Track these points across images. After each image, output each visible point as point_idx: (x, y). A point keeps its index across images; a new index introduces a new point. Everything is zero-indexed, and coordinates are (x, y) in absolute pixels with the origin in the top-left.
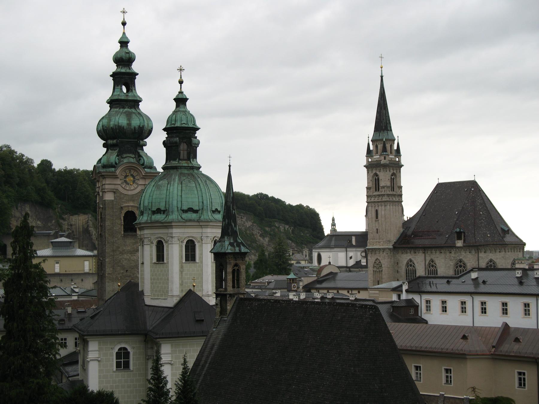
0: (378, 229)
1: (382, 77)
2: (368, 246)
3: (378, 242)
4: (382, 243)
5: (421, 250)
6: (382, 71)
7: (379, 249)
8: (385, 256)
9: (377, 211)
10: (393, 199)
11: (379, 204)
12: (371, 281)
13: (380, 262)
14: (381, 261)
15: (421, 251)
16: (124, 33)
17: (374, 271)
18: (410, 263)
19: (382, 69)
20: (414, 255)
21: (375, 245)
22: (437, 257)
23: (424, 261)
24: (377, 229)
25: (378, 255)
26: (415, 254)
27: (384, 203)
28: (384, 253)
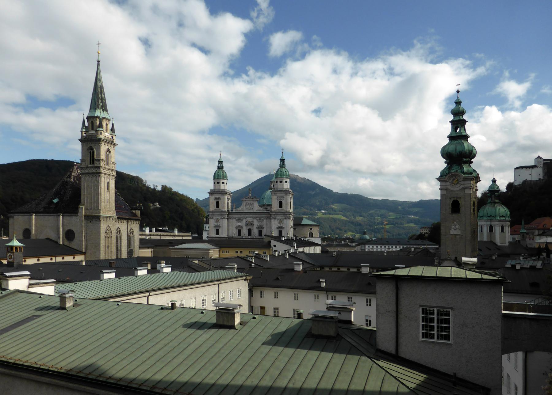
2: (101, 213)
3: (109, 211)
4: (112, 212)
5: (125, 220)
7: (110, 217)
8: (114, 224)
10: (85, 171)
13: (110, 229)
15: (125, 222)
16: (458, 97)
18: (119, 231)
20: (121, 224)
22: (134, 227)
25: (109, 222)
26: (121, 223)
28: (114, 222)
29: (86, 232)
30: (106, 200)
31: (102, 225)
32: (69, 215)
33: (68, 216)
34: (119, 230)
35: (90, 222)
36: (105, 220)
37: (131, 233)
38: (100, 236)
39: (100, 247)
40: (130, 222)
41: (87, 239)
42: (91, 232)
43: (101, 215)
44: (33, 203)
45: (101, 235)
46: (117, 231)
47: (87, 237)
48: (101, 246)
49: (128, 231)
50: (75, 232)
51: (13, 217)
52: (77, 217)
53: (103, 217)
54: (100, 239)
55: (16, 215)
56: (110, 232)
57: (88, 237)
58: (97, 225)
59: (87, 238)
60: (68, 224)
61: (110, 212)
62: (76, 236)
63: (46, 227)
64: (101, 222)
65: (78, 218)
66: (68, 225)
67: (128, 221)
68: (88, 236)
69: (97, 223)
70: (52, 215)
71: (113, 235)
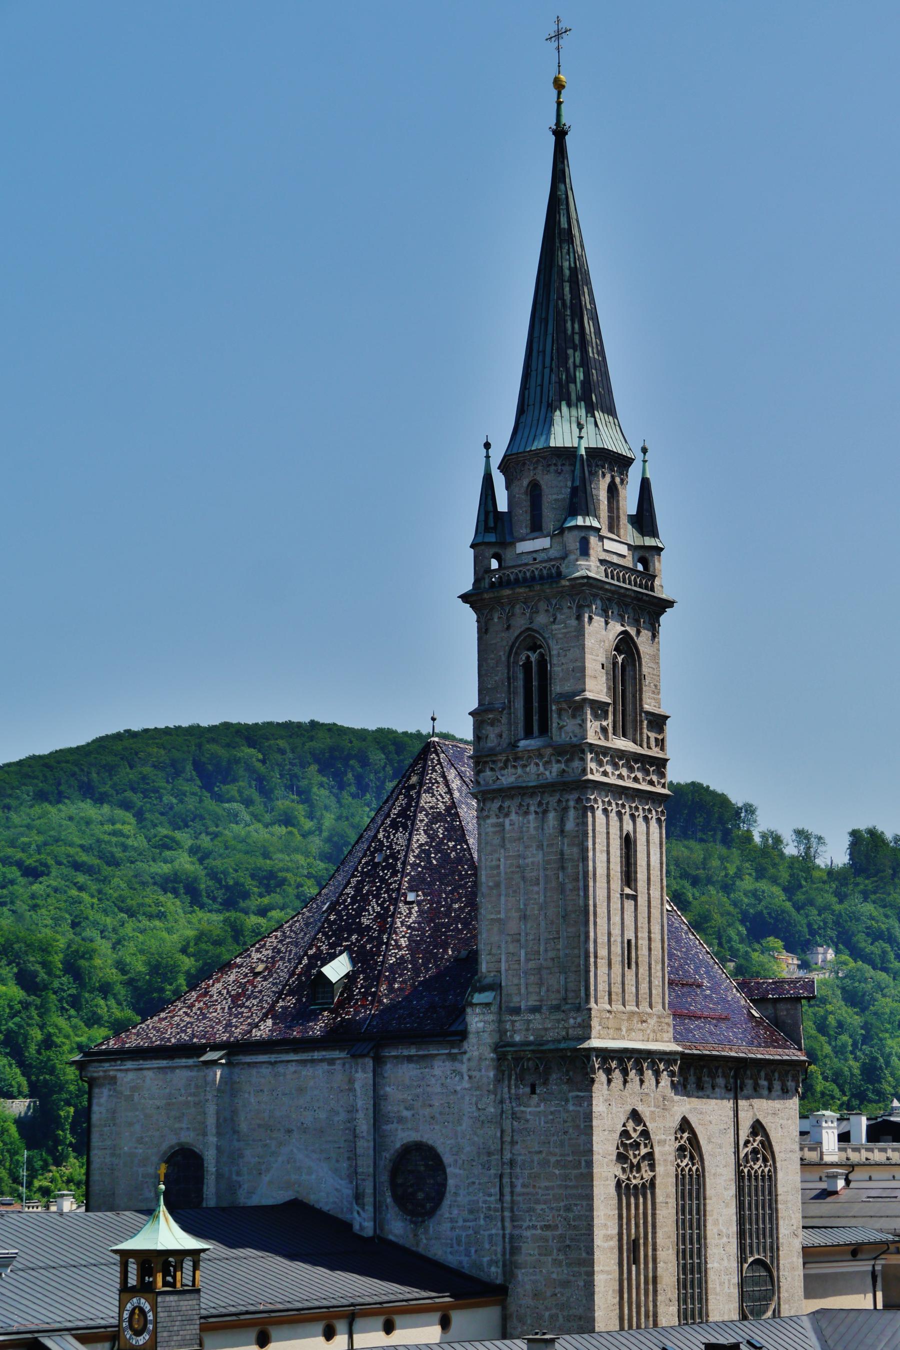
0: (633, 942)
1: (560, 134)
2: (594, 1033)
3: (635, 1019)
4: (652, 1021)
6: (559, 104)
8: (664, 1099)
9: (628, 843)
11: (547, 798)
12: (606, 1245)
13: (645, 1134)
14: (651, 1126)
17: (619, 1184)
19: (563, 91)
21: (624, 1032)
23: (731, 1132)
24: (629, 941)
27: (557, 796)
28: (662, 1083)
29: (507, 1156)
30: (617, 949)
31: (599, 1106)
32: (413, 1052)
33: (410, 1059)
34: (688, 1139)
35: (533, 1092)
36: (617, 1075)
37: (755, 1151)
38: (590, 1176)
39: (590, 1251)
40: (749, 1083)
41: (512, 1202)
42: (541, 1152)
43: (595, 1043)
44: (214, 990)
45: (596, 1170)
46: (677, 1145)
47: (512, 1185)
48: (598, 1241)
49: (741, 1143)
50: (447, 1159)
51: (115, 1077)
52: (457, 1065)
53: (606, 1055)
54: (590, 1197)
55: (129, 1065)
56: (644, 1151)
57: (519, 1189)
58: (571, 1108)
59: (512, 1193)
60: (407, 1109)
61: (643, 1022)
62: (451, 1182)
63: (289, 1131)
64: (596, 1087)
65: (464, 1068)
66: (407, 1114)
67: (735, 1077)
68: (519, 1183)
69: (571, 1094)
70: (317, 1055)
71: (659, 1169)
